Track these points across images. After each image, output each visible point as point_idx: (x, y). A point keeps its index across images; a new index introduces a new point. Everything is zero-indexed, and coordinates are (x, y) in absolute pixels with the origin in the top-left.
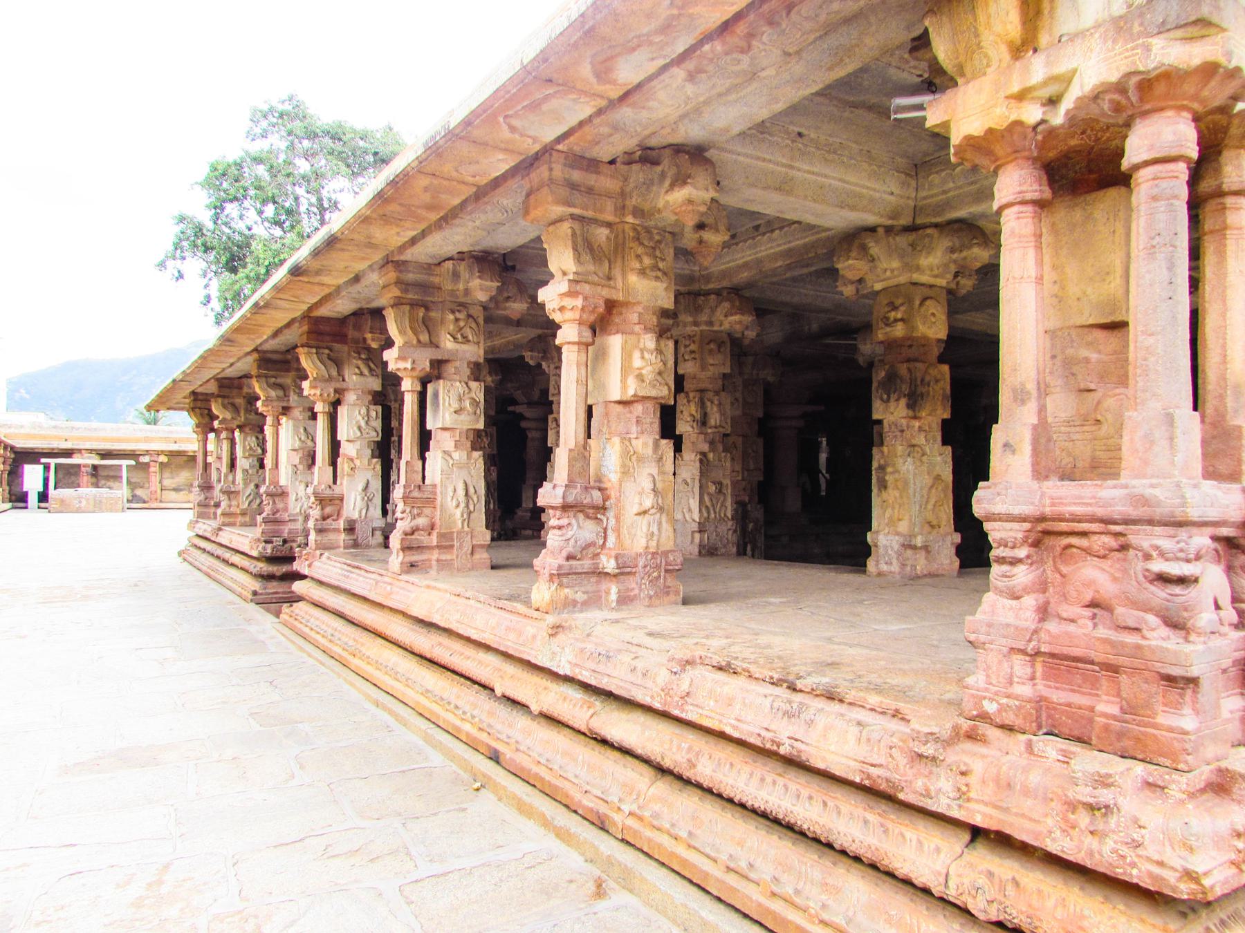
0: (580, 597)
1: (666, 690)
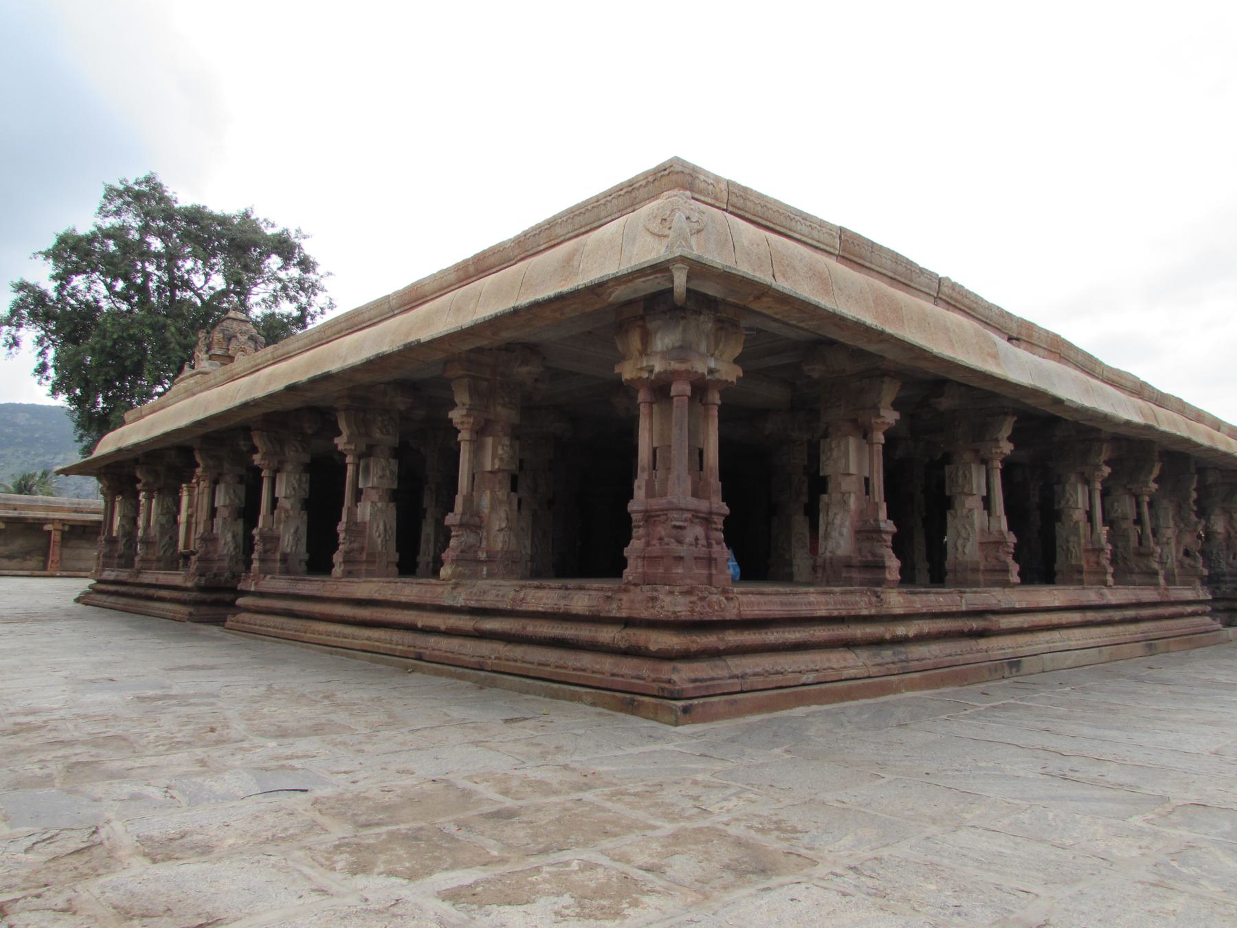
0: (467, 572)
1: (514, 600)
